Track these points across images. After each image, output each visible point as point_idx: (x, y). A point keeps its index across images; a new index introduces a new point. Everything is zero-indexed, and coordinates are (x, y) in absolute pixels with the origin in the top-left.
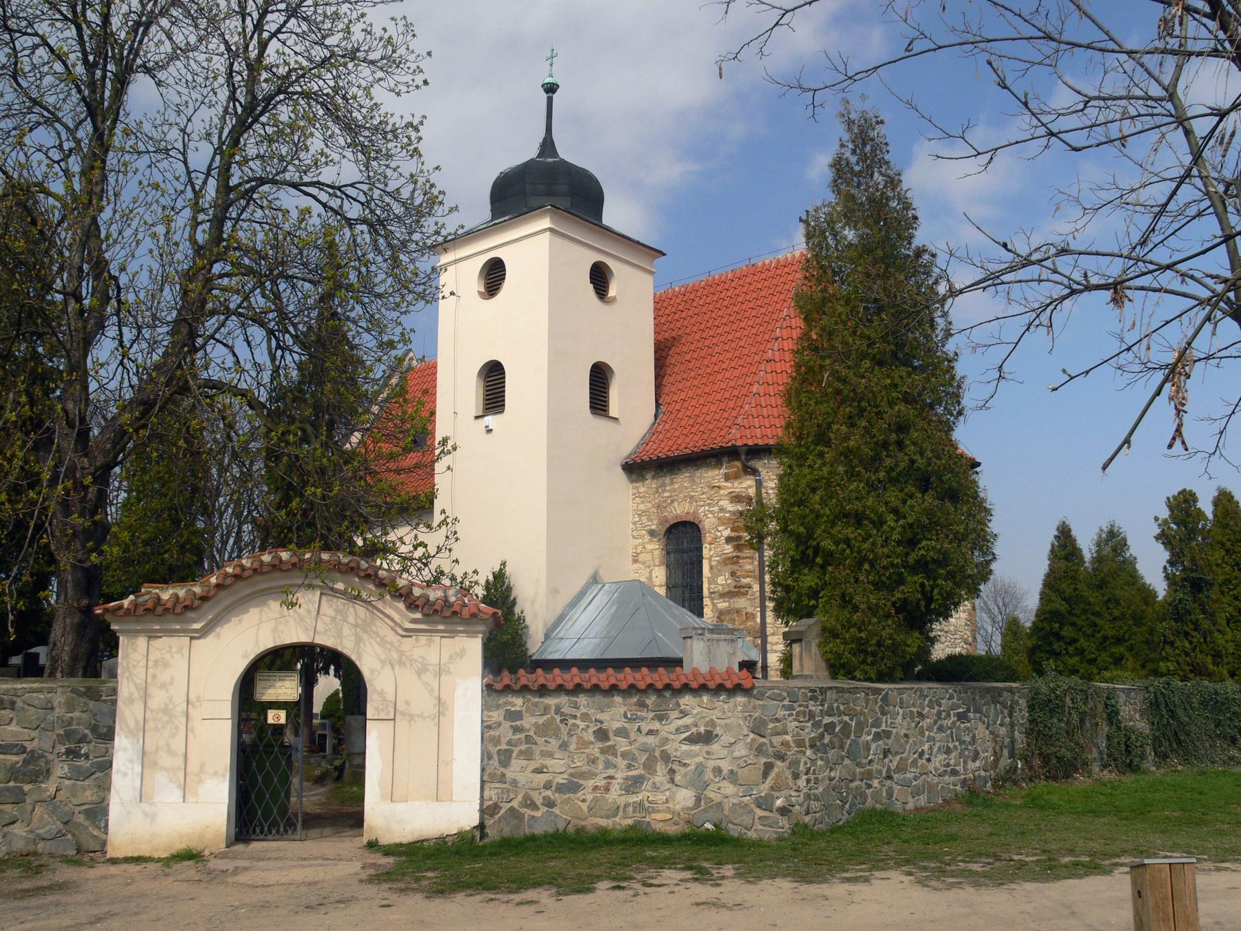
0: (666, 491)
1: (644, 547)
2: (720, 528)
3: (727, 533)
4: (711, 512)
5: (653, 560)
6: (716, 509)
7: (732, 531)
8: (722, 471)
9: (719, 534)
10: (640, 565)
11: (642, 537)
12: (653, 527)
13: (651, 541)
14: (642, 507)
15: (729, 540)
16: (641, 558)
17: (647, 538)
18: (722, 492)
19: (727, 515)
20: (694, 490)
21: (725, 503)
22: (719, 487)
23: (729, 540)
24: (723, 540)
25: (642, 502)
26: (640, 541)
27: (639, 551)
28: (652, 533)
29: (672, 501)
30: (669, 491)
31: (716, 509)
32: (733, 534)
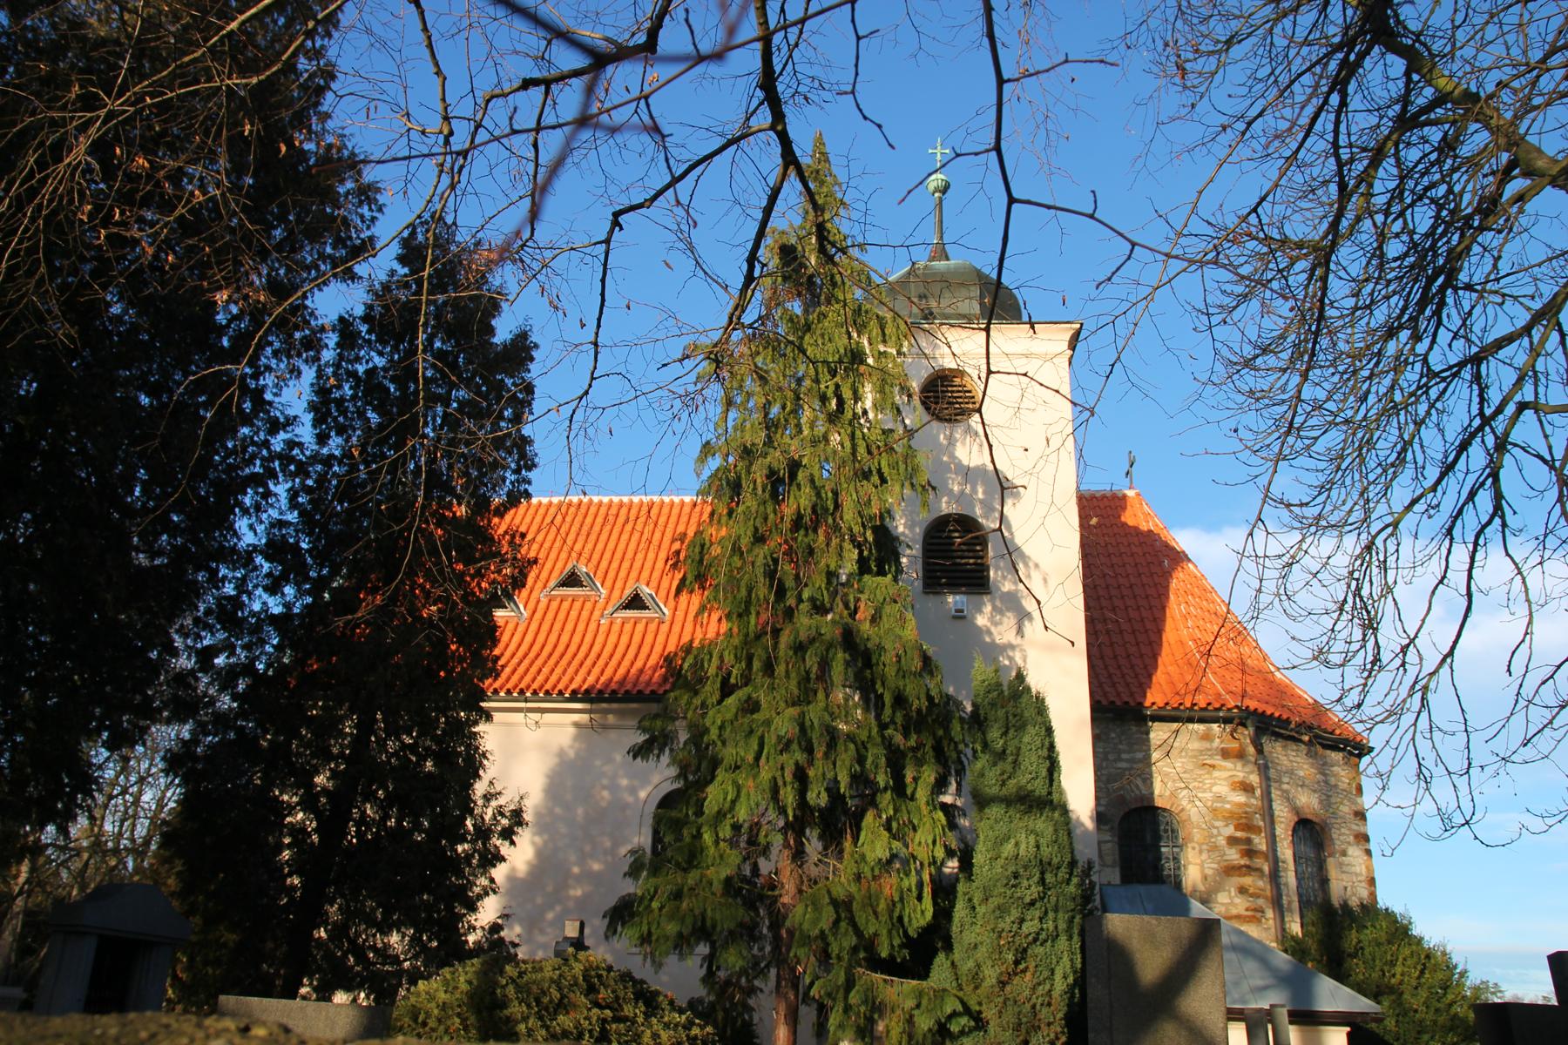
0: (1120, 760)
2: (1217, 824)
3: (1230, 830)
6: (1208, 795)
7: (1237, 828)
9: (1215, 831)
15: (1232, 841)
18: (1216, 774)
19: (1228, 806)
22: (1213, 766)
23: (1232, 841)
24: (1222, 841)
30: (1127, 761)
31: (1208, 795)
32: (1239, 834)
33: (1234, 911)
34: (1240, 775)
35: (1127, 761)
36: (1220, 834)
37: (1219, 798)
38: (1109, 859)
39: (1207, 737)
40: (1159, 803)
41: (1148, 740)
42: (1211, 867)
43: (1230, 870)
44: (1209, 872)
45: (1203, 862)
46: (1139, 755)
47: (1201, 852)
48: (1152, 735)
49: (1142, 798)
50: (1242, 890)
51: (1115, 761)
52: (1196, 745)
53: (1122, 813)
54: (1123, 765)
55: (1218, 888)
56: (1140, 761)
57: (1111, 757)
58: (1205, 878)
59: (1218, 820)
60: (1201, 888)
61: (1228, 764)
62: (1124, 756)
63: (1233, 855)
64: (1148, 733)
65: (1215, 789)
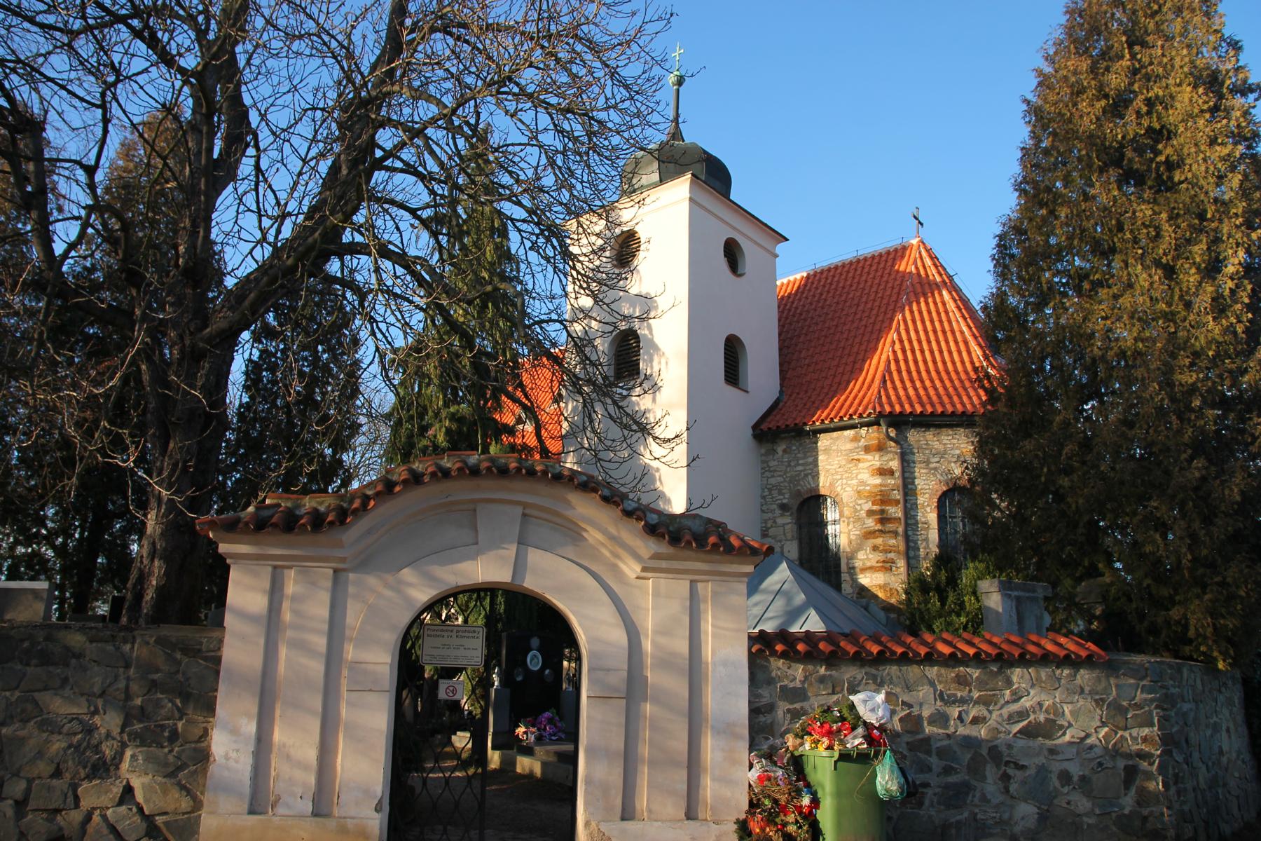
0: (799, 465)
1: (775, 522)
2: (860, 502)
3: (868, 506)
4: (849, 485)
5: (784, 534)
6: (855, 482)
7: (873, 504)
9: (858, 508)
11: (772, 511)
13: (782, 515)
14: (772, 481)
16: (772, 532)
17: (778, 512)
18: (861, 465)
20: (830, 464)
23: (870, 513)
24: (863, 514)
25: (773, 476)
26: (770, 515)
27: (769, 525)
28: (784, 507)
29: (806, 475)
30: (802, 465)
31: (855, 482)
32: (875, 508)
33: (868, 564)
34: (877, 464)
35: (802, 465)
36: (862, 509)
37: (862, 483)
38: (789, 536)
39: (856, 439)
40: (822, 492)
41: (817, 447)
42: (855, 533)
43: (869, 534)
44: (853, 537)
45: (849, 531)
46: (810, 460)
47: (848, 525)
48: (819, 444)
49: (810, 490)
50: (875, 548)
51: (795, 466)
52: (849, 446)
53: (798, 502)
54: (800, 468)
55: (860, 548)
56: (811, 463)
57: (792, 464)
58: (850, 542)
59: (861, 499)
60: (848, 550)
61: (869, 457)
62: (801, 462)
63: (871, 523)
64: (816, 443)
65: (859, 477)
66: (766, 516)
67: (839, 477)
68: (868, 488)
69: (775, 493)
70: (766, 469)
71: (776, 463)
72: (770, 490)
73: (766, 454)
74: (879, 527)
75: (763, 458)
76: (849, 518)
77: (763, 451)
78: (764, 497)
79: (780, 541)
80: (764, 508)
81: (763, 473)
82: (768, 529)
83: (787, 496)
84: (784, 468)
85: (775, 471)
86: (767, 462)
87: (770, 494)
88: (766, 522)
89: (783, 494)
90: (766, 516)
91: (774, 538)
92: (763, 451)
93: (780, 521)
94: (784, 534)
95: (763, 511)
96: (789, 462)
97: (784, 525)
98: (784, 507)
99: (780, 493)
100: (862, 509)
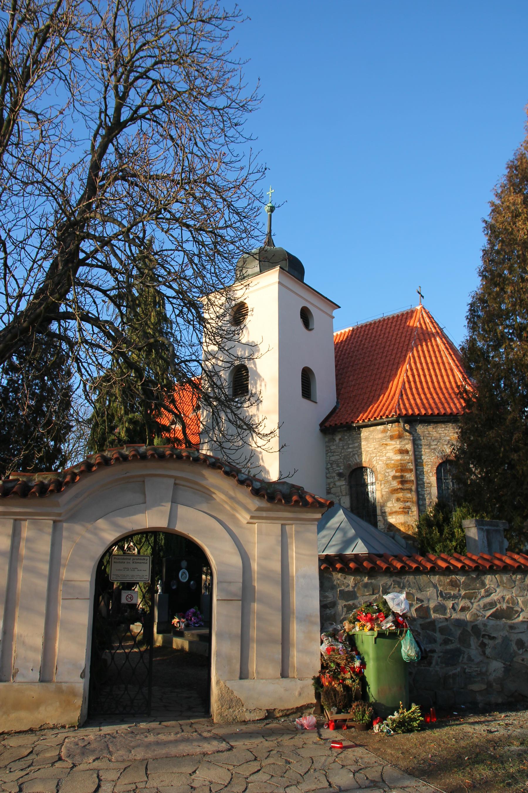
0: (349, 448)
1: (335, 484)
2: (388, 471)
3: (393, 473)
4: (381, 460)
8: (388, 434)
9: (387, 474)
10: (332, 496)
12: (341, 471)
13: (339, 480)
14: (333, 458)
16: (333, 490)
17: (337, 478)
18: (388, 448)
20: (368, 447)
21: (391, 454)
22: (386, 444)
23: (395, 478)
24: (390, 478)
25: (333, 456)
26: (332, 480)
27: (331, 486)
28: (340, 475)
29: (354, 455)
31: (384, 458)
32: (397, 474)
36: (389, 475)
38: (344, 493)
42: (386, 490)
45: (382, 489)
48: (362, 435)
49: (357, 464)
51: (347, 449)
54: (350, 450)
57: (345, 447)
59: (388, 469)
62: (350, 446)
66: (329, 481)
67: (374, 455)
68: (393, 462)
69: (335, 466)
70: (328, 451)
71: (335, 447)
72: (331, 464)
73: (329, 441)
74: (400, 486)
75: (327, 444)
76: (381, 481)
77: (327, 439)
78: (327, 469)
79: (338, 496)
80: (328, 475)
81: (327, 454)
82: (330, 489)
83: (342, 468)
84: (339, 450)
85: (334, 452)
86: (329, 447)
87: (332, 467)
88: (329, 484)
89: (340, 467)
90: (329, 481)
91: (334, 494)
92: (327, 439)
93: (338, 484)
94: (341, 492)
95: (327, 478)
96: (343, 446)
97: (340, 486)
98: (340, 475)
99: (338, 466)
100: (389, 475)
